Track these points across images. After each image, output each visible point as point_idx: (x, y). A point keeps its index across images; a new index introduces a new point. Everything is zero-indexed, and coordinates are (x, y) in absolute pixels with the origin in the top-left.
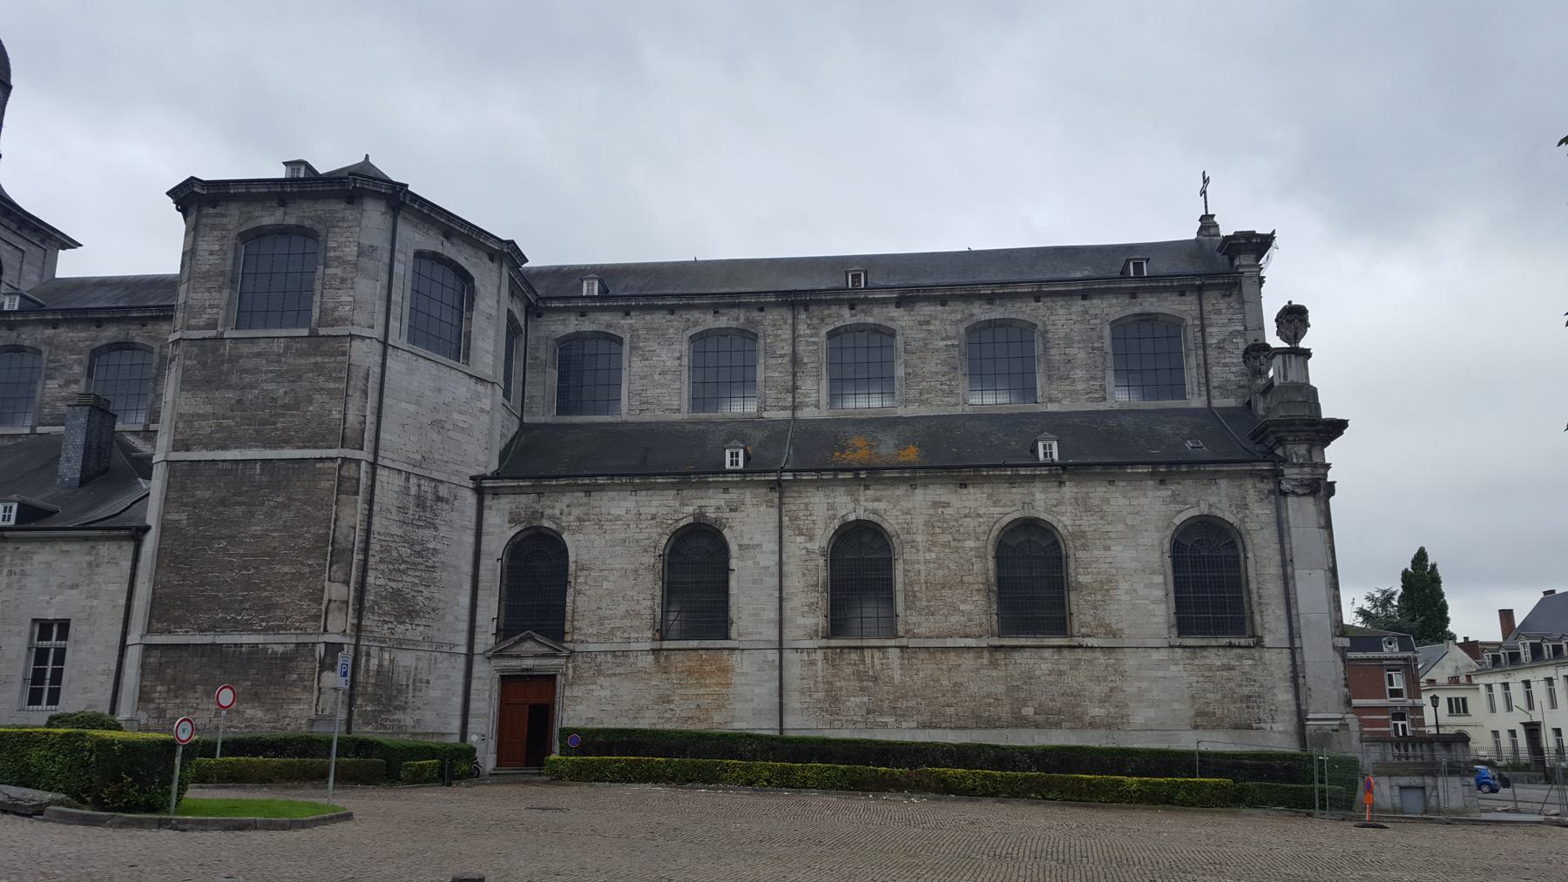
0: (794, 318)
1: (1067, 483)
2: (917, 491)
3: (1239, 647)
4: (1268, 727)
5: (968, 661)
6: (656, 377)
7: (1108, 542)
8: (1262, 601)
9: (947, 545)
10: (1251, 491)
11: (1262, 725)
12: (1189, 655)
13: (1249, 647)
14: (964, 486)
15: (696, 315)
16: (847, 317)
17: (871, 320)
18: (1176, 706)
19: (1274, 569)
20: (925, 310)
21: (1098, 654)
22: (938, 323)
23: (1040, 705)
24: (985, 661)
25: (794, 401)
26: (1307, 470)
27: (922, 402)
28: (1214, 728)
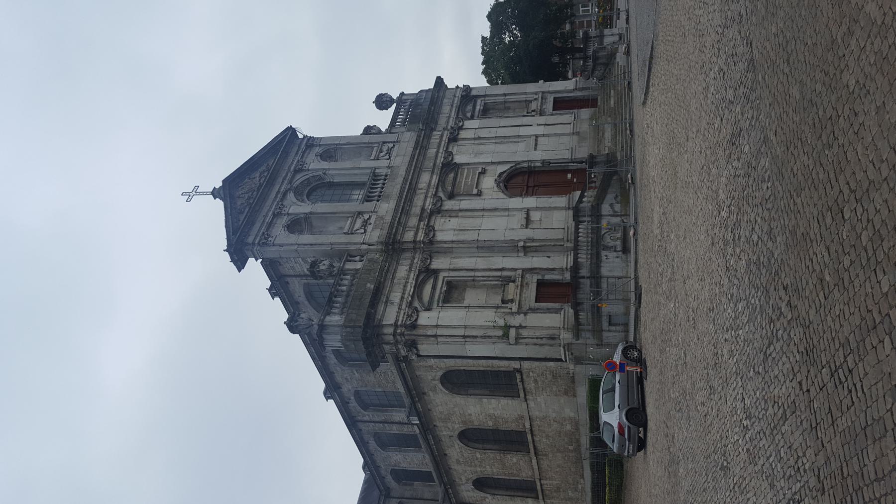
0: (361, 421)
1: (435, 424)
2: (453, 467)
3: (522, 377)
4: (571, 372)
5: (545, 463)
6: (408, 460)
7: (467, 414)
8: (491, 365)
9: (481, 462)
10: (421, 364)
11: (571, 373)
12: (530, 395)
13: (522, 375)
14: (446, 455)
15: (371, 448)
16: (353, 404)
17: (352, 398)
18: (562, 401)
19: (470, 361)
20: (339, 379)
21: (535, 423)
22: (345, 376)
23: (567, 443)
24: (544, 458)
25: (408, 424)
26: (400, 347)
27: (394, 382)
28: (574, 390)
